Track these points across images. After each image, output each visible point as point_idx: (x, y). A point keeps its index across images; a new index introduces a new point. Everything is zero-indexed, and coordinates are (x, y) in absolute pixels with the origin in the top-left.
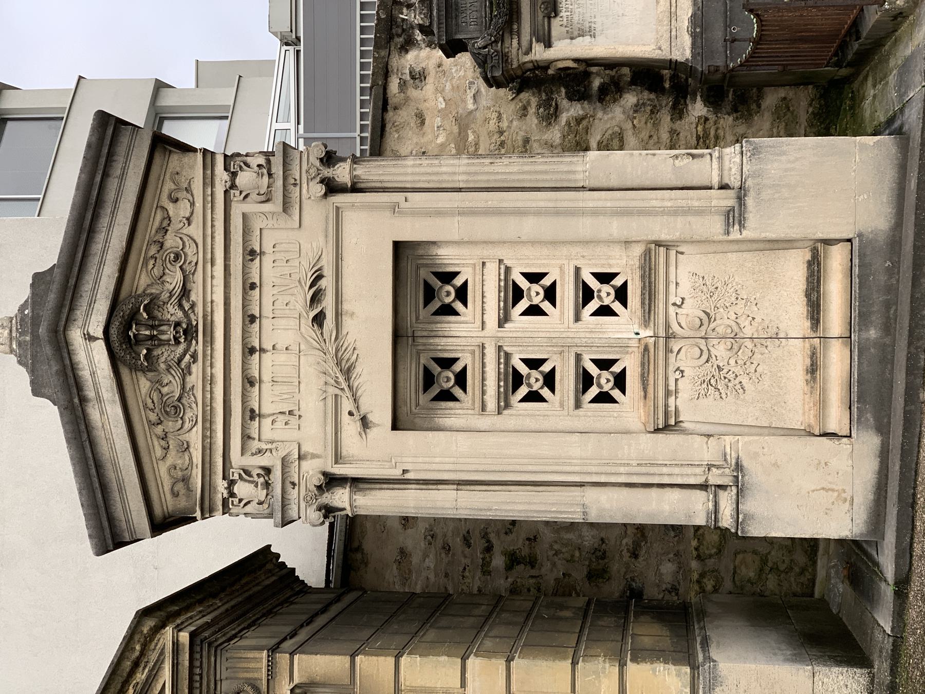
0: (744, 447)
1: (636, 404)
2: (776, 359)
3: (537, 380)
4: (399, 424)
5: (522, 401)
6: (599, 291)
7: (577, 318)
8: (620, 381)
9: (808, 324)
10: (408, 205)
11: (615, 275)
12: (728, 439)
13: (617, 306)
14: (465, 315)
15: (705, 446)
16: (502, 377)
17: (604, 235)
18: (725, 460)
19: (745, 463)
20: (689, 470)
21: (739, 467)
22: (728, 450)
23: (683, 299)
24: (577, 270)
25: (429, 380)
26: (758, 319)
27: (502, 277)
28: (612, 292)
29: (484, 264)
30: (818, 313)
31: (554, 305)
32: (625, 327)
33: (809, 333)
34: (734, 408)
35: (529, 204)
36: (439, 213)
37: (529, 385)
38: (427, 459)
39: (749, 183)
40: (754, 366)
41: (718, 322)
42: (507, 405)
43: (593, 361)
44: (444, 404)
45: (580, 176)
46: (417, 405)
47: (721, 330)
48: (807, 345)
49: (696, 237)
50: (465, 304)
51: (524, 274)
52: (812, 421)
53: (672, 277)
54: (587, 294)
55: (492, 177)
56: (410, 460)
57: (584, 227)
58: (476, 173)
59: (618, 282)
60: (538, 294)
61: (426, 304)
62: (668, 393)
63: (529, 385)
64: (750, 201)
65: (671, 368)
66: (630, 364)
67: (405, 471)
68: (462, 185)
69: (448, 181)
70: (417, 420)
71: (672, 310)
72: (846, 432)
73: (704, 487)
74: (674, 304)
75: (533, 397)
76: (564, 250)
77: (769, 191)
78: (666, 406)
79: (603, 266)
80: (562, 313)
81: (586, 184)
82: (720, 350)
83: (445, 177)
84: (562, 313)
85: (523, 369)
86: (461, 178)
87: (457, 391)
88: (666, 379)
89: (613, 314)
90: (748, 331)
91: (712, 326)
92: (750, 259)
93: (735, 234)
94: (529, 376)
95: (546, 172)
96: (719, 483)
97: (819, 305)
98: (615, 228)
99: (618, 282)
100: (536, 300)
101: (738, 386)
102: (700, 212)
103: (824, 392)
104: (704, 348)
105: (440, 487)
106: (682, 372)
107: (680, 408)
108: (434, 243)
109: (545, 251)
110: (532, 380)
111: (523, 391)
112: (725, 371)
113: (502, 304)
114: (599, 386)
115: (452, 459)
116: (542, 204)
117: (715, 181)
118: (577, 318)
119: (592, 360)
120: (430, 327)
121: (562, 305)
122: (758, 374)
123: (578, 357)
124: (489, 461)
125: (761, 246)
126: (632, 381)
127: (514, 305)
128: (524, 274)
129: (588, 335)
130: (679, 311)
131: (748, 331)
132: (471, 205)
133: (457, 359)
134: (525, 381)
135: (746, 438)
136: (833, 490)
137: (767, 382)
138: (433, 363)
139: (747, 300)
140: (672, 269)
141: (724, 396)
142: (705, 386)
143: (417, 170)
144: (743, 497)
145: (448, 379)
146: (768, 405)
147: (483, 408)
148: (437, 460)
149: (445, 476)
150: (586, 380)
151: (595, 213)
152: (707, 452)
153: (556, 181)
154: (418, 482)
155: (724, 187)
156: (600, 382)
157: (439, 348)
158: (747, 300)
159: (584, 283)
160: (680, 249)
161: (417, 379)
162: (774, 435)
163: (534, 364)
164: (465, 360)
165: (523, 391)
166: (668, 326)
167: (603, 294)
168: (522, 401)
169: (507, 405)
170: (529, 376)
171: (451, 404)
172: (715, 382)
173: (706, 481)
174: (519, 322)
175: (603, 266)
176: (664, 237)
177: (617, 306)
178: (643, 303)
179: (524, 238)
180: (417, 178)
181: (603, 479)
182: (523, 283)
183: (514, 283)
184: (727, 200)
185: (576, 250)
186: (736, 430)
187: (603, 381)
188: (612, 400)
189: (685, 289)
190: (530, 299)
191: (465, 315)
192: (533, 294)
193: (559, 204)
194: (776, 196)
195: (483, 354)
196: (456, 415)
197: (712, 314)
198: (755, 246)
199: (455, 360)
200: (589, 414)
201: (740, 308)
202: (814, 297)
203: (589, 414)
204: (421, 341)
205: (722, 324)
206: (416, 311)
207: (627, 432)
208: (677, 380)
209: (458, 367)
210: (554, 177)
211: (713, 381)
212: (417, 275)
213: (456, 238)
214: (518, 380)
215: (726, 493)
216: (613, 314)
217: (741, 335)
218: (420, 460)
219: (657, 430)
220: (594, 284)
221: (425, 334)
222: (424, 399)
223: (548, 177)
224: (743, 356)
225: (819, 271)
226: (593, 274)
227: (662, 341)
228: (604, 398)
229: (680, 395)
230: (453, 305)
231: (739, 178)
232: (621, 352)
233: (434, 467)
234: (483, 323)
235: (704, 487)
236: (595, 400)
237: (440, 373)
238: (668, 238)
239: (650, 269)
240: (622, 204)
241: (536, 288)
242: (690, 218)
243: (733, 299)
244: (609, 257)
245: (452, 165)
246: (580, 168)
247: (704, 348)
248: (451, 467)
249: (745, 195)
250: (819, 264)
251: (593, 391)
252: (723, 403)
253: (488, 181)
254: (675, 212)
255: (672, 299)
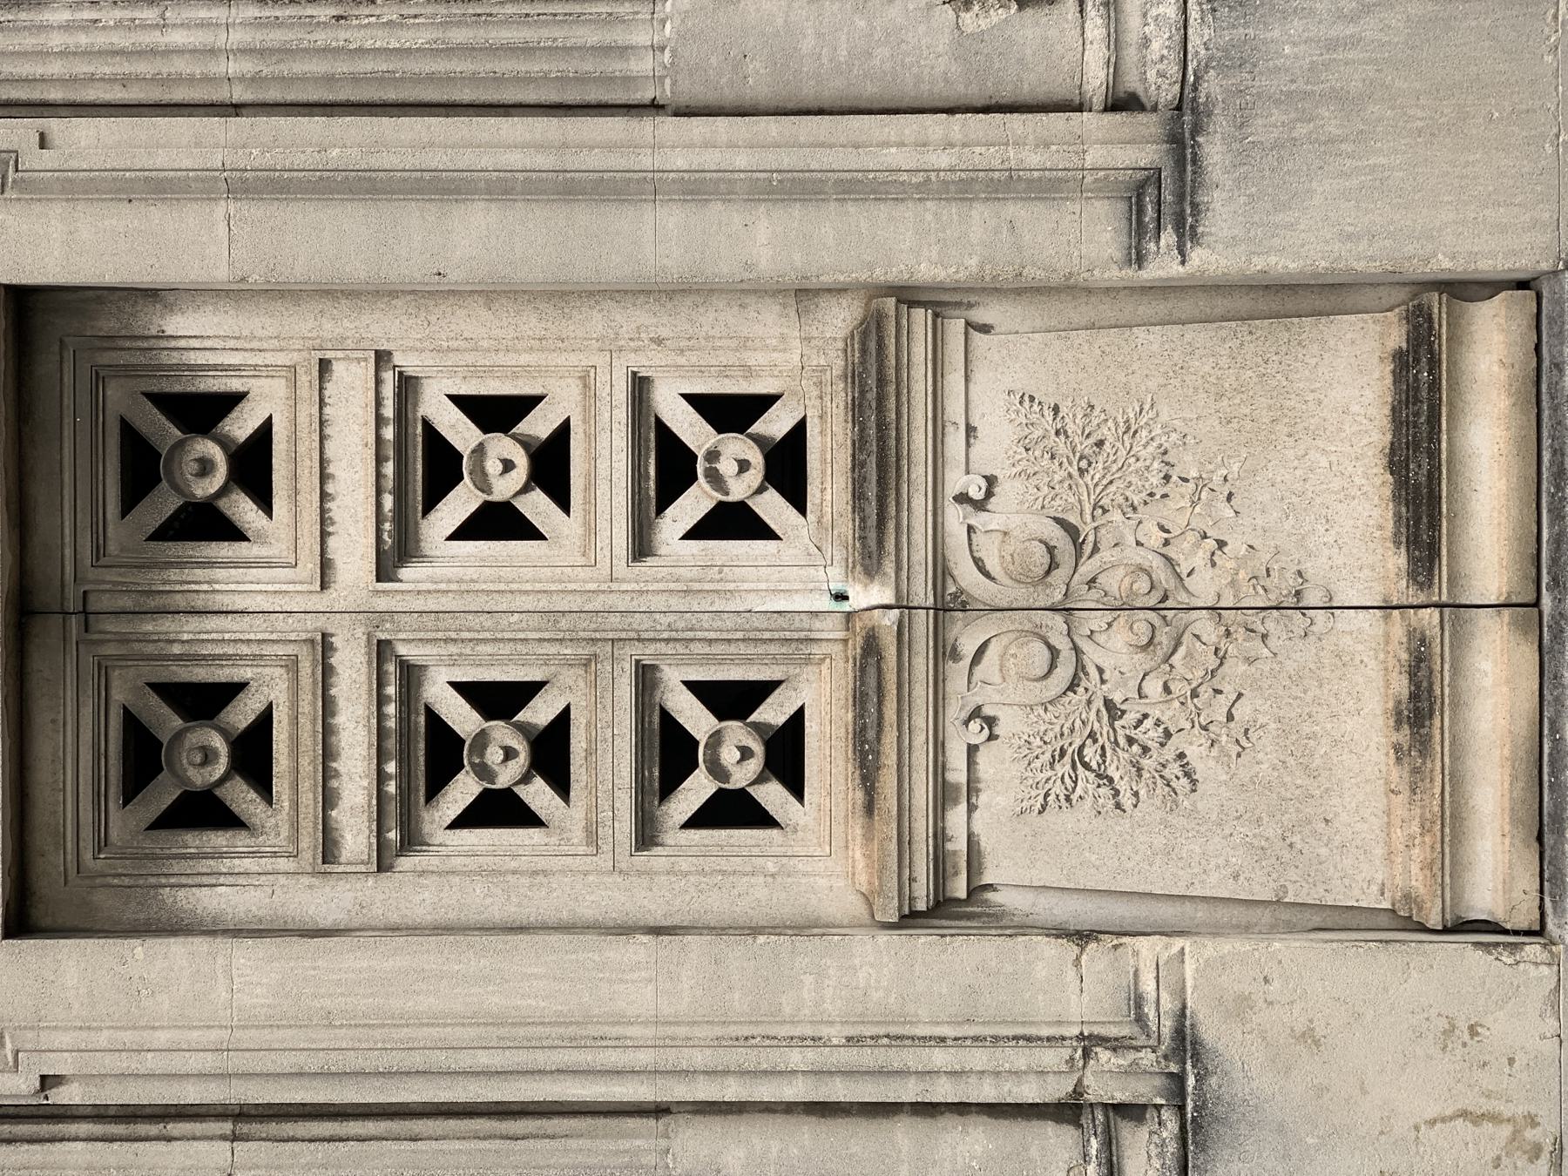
0: (1202, 974)
1: (838, 830)
2: (1296, 679)
3: (509, 754)
4: (39, 915)
5: (460, 823)
6: (713, 455)
7: (642, 547)
8: (785, 754)
9: (1398, 561)
10: (48, 158)
11: (765, 402)
12: (1147, 949)
13: (772, 507)
14: (262, 538)
15: (1071, 973)
16: (391, 744)
17: (725, 268)
18: (1140, 1019)
19: (1210, 1030)
20: (1020, 1058)
21: (1185, 1043)
22: (1148, 986)
23: (991, 481)
24: (640, 387)
25: (142, 756)
26: (1236, 546)
27: (389, 411)
28: (756, 458)
29: (324, 366)
30: (1434, 525)
31: (563, 502)
32: (798, 574)
33: (1402, 591)
34: (1159, 841)
35: (466, 159)
36: (160, 188)
37: (484, 772)
38: (128, 1037)
39: (1212, 86)
40: (1223, 702)
41: (1106, 555)
42: (411, 840)
43: (694, 687)
44: (194, 840)
45: (642, 65)
46: (102, 843)
47: (1114, 582)
48: (1398, 631)
49: (1032, 273)
50: (264, 501)
51: (460, 401)
52: (1418, 882)
53: (954, 409)
54: (672, 467)
55: (342, 67)
56: (65, 1039)
57: (660, 238)
58: (285, 52)
59: (775, 424)
60: (508, 466)
61: (130, 501)
62: (944, 795)
63: (484, 772)
64: (1214, 151)
65: (954, 712)
66: (819, 697)
67: (46, 1082)
68: (239, 94)
69: (191, 80)
70: (100, 898)
71: (955, 518)
72: (1525, 917)
73: (1068, 1111)
74: (963, 498)
75: (500, 809)
76: (595, 322)
77: (1277, 116)
78: (940, 836)
79: (724, 371)
80: (591, 530)
81: (665, 93)
82: (1114, 650)
83: (181, 66)
84: (591, 530)
85: (463, 718)
86: (234, 67)
87: (241, 797)
88: (940, 746)
89: (758, 530)
90: (1204, 587)
91: (1087, 568)
92: (1208, 350)
93: (1163, 265)
94: (482, 739)
95: (526, 50)
96: (1120, 1097)
97: (1434, 499)
98: (765, 240)
99: (775, 424)
100: (504, 488)
101: (1174, 769)
102: (1045, 188)
103: (1456, 782)
104: (1062, 644)
105: (175, 1128)
106: (991, 722)
107: (985, 843)
108: (151, 294)
109: (531, 323)
110: (494, 755)
111: (463, 791)
112: (1131, 718)
113: (388, 502)
114: (718, 771)
115: (214, 1036)
116: (515, 159)
117: (1096, 78)
118: (642, 547)
119: (691, 686)
120: (155, 579)
121: (591, 501)
122: (1236, 728)
123: (646, 678)
124: (343, 1038)
125: (1243, 303)
126: (825, 753)
127: (430, 504)
128: (460, 401)
129: (676, 603)
130: (978, 519)
131: (1204, 587)
132: (267, 160)
133: (238, 688)
134: (465, 758)
135: (1211, 948)
136: (1495, 1118)
137: (1266, 755)
138: (154, 700)
139: (1201, 483)
140: (954, 381)
141: (1126, 800)
142: (1064, 768)
143: (83, 39)
144: (1202, 1147)
145: (208, 756)
146: (1271, 830)
147: (329, 849)
148: (162, 1038)
149: (192, 1094)
150: (671, 754)
151: (697, 189)
152: (1074, 991)
153: (562, 80)
154: (99, 1114)
155: (1122, 103)
156: (715, 755)
157: (177, 649)
158: (1201, 483)
159: (663, 430)
160: (979, 316)
161: (99, 755)
162: (1291, 928)
163: (501, 700)
164: (269, 689)
165: (463, 791)
166: (941, 571)
167: (727, 467)
168: (460, 823)
169: (411, 840)
170: (482, 739)
171: (218, 839)
172: (1099, 754)
173: (1078, 1091)
174: (449, 561)
175: (724, 371)
176: (927, 270)
177: (772, 507)
178: (858, 496)
179: (455, 276)
180: (83, 68)
181: (732, 1091)
182: (461, 432)
183: (429, 430)
184: (1130, 147)
185: (632, 319)
186: (1166, 913)
187: (729, 755)
188: (761, 818)
189: (997, 444)
190: (483, 484)
191: (262, 538)
192: (493, 466)
193: (573, 161)
194: (1302, 130)
195: (327, 671)
196: (240, 877)
197: (1086, 529)
198: (1222, 304)
199: (234, 690)
200: (684, 864)
201: (1176, 510)
202: (1418, 472)
203: (684, 864)
204: (111, 626)
205: (1119, 564)
206: (94, 525)
207: (805, 927)
208: (972, 750)
209: (241, 714)
210: (552, 67)
211: (1090, 754)
212: (97, 406)
213: (221, 274)
214: (445, 753)
215: (1143, 1133)
216: (758, 530)
217: (1183, 598)
218: (103, 1039)
219: (910, 919)
220: (693, 431)
221: (126, 602)
222: (125, 823)
223: (536, 67)
224: (1188, 666)
225: (1435, 386)
226: (693, 400)
227: (922, 622)
228: (732, 810)
229: (983, 799)
230: (223, 504)
231: (1174, 70)
232: (788, 660)
233: (152, 1062)
234: (325, 565)
235: (1068, 1111)
236: (702, 819)
237: (179, 736)
238: (941, 274)
239: (882, 382)
240: (787, 159)
241: (502, 446)
242: (1012, 210)
243: (1155, 479)
244: (745, 343)
245: (203, 25)
246: (641, 37)
247: (1062, 644)
248: (209, 1062)
249: (1197, 129)
250: (1434, 363)
251: (697, 789)
252: (1126, 823)
253: (329, 79)
254: (965, 188)
255: (956, 481)
